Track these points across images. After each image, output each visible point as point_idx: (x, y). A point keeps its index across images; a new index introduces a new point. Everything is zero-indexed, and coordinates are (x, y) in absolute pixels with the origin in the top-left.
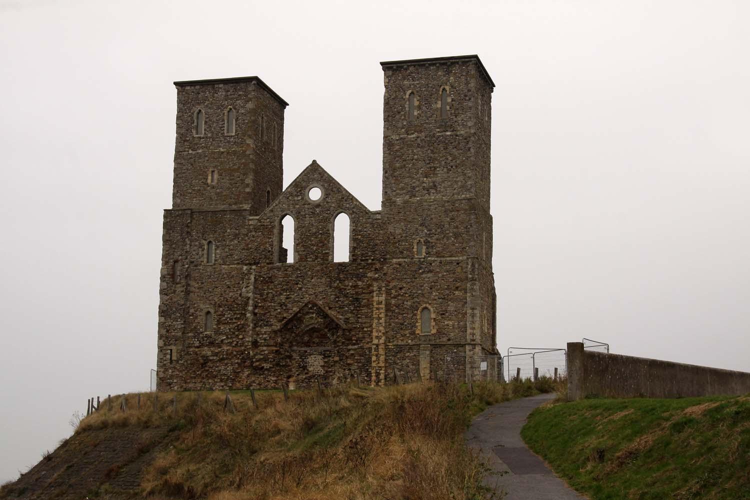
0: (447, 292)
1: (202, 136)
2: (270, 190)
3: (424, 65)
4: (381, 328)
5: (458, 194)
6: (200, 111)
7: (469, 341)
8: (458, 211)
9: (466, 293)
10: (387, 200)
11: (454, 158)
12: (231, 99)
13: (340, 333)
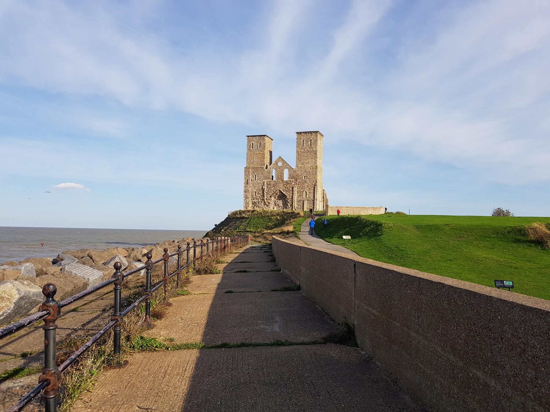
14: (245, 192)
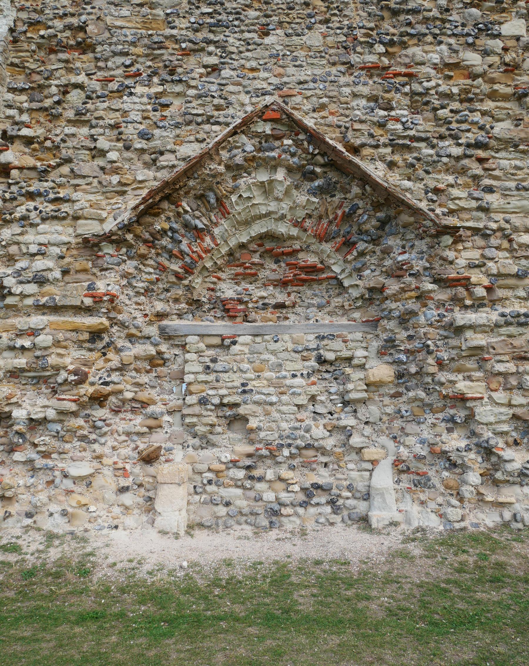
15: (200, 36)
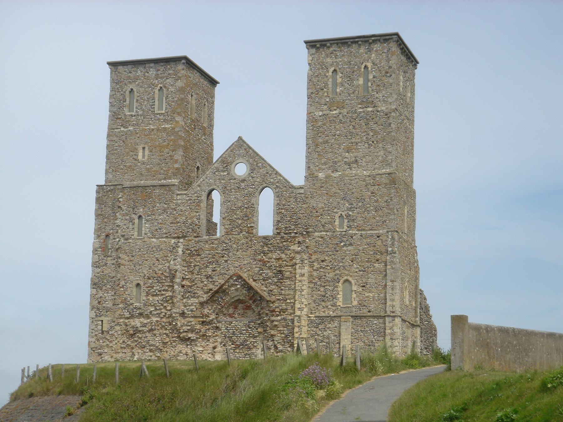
0: (369, 264)
1: (133, 114)
2: (200, 166)
3: (347, 43)
4: (303, 300)
5: (379, 169)
6: (132, 89)
7: (388, 313)
8: (379, 185)
9: (386, 265)
10: (310, 175)
11: (376, 133)
12: (161, 78)
13: (264, 304)
14: (95, 285)
15: (224, 252)
